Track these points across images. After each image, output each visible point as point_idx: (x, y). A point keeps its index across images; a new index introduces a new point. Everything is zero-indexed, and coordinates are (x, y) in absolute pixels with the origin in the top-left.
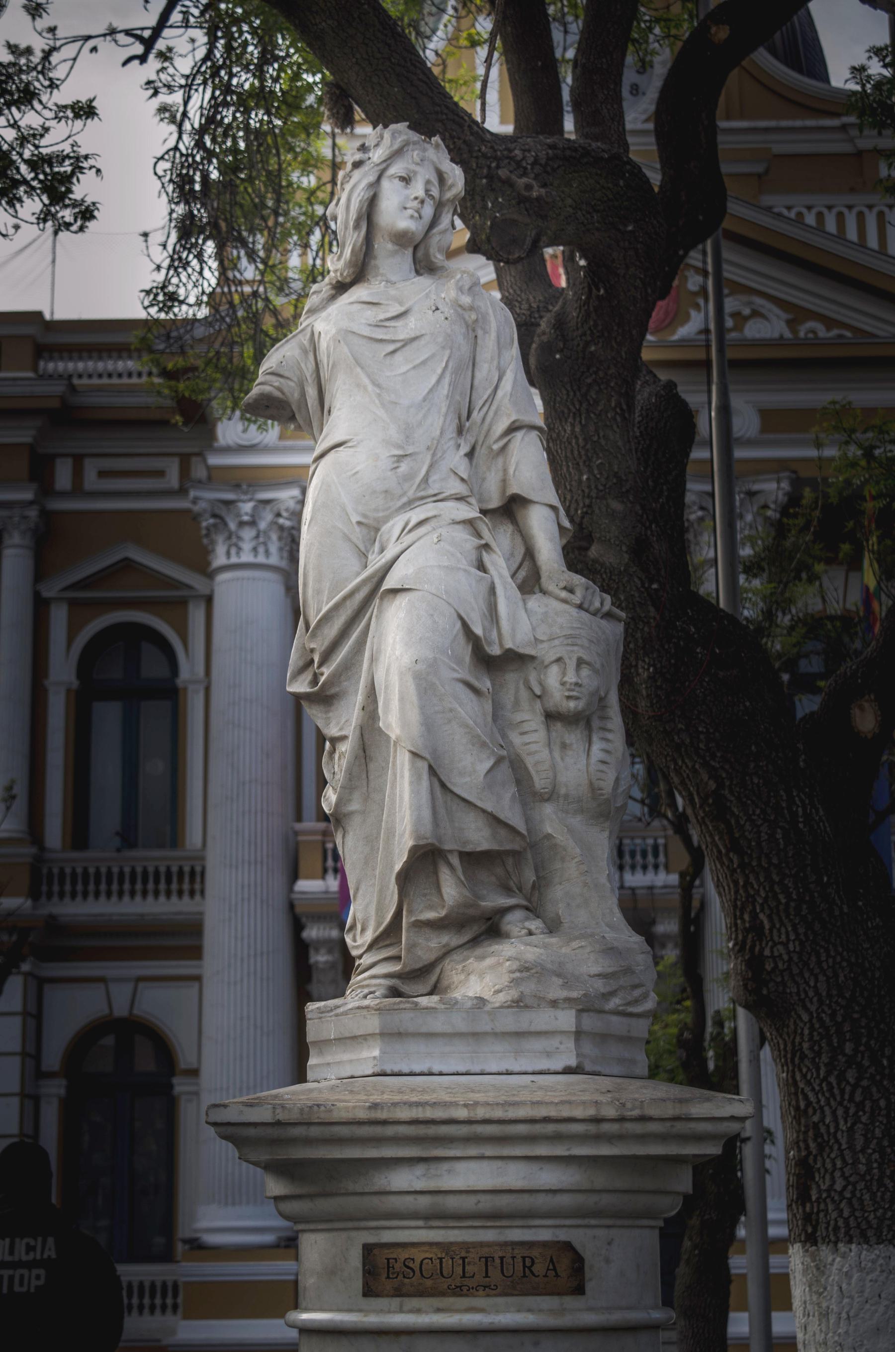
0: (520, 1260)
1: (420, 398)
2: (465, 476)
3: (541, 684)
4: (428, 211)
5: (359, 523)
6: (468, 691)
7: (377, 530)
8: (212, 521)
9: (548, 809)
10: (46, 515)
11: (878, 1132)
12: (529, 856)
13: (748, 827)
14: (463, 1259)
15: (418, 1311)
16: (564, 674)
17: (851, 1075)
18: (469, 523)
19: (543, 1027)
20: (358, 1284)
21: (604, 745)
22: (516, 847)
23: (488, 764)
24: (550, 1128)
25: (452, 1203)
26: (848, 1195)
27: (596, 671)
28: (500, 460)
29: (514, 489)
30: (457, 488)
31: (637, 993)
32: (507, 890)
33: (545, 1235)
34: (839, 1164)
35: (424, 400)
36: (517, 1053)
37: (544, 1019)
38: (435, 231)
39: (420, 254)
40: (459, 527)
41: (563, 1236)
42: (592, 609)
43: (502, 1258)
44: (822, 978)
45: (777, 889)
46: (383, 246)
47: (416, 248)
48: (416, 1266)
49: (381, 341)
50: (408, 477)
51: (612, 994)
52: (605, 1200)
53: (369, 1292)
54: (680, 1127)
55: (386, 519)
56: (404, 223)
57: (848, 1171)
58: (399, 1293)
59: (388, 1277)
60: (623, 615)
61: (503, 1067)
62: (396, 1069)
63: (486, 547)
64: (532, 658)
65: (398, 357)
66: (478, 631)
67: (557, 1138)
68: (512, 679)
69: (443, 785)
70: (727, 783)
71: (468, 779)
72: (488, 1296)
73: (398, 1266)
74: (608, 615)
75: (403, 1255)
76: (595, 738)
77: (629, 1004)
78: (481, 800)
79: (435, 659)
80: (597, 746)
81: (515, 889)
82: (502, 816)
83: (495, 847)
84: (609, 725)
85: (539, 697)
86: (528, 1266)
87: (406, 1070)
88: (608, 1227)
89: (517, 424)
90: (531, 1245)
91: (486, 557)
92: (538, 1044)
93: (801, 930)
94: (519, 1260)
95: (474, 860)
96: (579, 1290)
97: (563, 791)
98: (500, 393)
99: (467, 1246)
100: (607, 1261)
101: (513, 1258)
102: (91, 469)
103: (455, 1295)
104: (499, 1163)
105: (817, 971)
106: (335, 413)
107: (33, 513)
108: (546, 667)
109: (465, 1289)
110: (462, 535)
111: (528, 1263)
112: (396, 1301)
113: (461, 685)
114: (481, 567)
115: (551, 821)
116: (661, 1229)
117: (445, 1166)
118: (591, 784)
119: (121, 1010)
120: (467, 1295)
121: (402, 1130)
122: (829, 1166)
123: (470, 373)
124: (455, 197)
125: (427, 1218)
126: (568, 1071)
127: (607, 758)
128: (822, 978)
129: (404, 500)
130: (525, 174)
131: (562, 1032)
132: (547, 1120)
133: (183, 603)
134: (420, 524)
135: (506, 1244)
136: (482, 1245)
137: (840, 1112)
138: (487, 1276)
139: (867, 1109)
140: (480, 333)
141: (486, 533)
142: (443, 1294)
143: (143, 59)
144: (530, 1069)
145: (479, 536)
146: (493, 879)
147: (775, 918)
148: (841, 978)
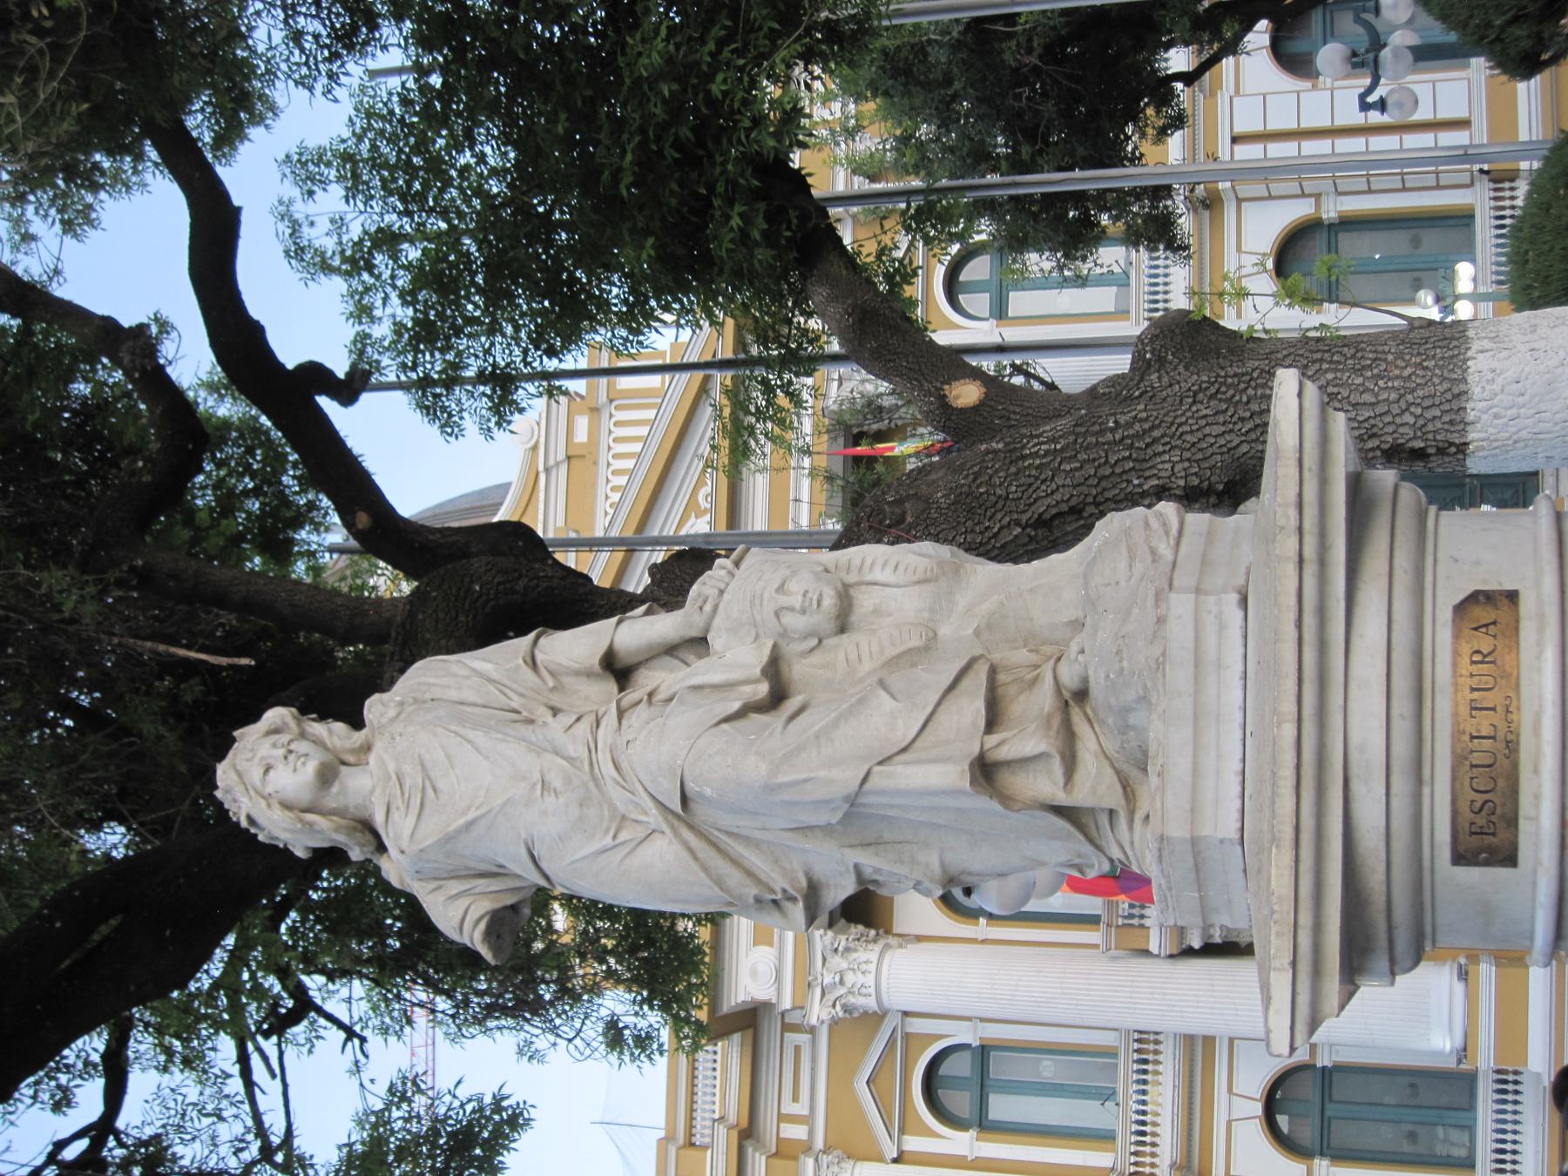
0: (1474, 667)
3: (806, 637)
4: (302, 747)
5: (615, 837)
7: (624, 817)
8: (838, 1007)
9: (945, 631)
10: (827, 1150)
11: (1359, 380)
12: (996, 656)
13: (1057, 496)
14: (1473, 737)
15: (1537, 797)
16: (791, 609)
18: (621, 714)
19: (1191, 634)
20: (1501, 873)
21: (878, 568)
25: (1402, 748)
26: (1419, 411)
27: (794, 573)
29: (595, 661)
30: (584, 728)
31: (1154, 524)
32: (1034, 681)
33: (1445, 634)
34: (1388, 419)
35: (487, 758)
36: (1219, 666)
37: (1179, 632)
39: (351, 759)
41: (1445, 614)
43: (1473, 690)
44: (1207, 430)
45: (1118, 470)
46: (332, 800)
48: (1480, 798)
49: (422, 804)
50: (568, 780)
51: (1153, 552)
52: (1403, 560)
53: (1511, 860)
54: (1310, 460)
56: (310, 769)
57: (1395, 410)
58: (1512, 822)
59: (1493, 834)
60: (741, 547)
61: (1239, 684)
62: (1236, 815)
63: (650, 695)
64: (775, 646)
65: (441, 785)
66: (736, 706)
67: (1322, 611)
68: (799, 670)
69: (904, 750)
70: (1015, 516)
72: (1518, 709)
73: (1481, 821)
74: (737, 564)
75: (1466, 815)
76: (869, 578)
77: (1167, 533)
80: (878, 575)
83: (983, 691)
84: (857, 562)
85: (820, 641)
86: (1484, 658)
87: (1238, 803)
88: (1435, 561)
89: (529, 659)
90: (1456, 653)
92: (1210, 639)
93: (1161, 449)
94: (1475, 669)
95: (993, 721)
96: (1512, 596)
97: (926, 615)
98: (495, 675)
99: (1457, 734)
100: (1477, 563)
101: (1472, 675)
104: (1353, 686)
105: (1200, 435)
106: (502, 861)
109: (1510, 737)
110: (635, 718)
111: (1477, 658)
112: (1523, 825)
113: (791, 725)
115: (958, 631)
116: (1440, 509)
117: (1354, 756)
118: (919, 582)
119: (1258, 1109)
120: (1518, 735)
122: (1390, 429)
123: (469, 709)
125: (1419, 780)
127: (892, 564)
128: (1207, 430)
129: (591, 785)
132: (1299, 624)
135: (1455, 684)
136: (1455, 715)
138: (1493, 709)
139: (1336, 390)
140: (428, 696)
143: (363, 1040)
144: (1241, 650)
146: (1022, 698)
147: (1148, 473)
148: (1208, 412)
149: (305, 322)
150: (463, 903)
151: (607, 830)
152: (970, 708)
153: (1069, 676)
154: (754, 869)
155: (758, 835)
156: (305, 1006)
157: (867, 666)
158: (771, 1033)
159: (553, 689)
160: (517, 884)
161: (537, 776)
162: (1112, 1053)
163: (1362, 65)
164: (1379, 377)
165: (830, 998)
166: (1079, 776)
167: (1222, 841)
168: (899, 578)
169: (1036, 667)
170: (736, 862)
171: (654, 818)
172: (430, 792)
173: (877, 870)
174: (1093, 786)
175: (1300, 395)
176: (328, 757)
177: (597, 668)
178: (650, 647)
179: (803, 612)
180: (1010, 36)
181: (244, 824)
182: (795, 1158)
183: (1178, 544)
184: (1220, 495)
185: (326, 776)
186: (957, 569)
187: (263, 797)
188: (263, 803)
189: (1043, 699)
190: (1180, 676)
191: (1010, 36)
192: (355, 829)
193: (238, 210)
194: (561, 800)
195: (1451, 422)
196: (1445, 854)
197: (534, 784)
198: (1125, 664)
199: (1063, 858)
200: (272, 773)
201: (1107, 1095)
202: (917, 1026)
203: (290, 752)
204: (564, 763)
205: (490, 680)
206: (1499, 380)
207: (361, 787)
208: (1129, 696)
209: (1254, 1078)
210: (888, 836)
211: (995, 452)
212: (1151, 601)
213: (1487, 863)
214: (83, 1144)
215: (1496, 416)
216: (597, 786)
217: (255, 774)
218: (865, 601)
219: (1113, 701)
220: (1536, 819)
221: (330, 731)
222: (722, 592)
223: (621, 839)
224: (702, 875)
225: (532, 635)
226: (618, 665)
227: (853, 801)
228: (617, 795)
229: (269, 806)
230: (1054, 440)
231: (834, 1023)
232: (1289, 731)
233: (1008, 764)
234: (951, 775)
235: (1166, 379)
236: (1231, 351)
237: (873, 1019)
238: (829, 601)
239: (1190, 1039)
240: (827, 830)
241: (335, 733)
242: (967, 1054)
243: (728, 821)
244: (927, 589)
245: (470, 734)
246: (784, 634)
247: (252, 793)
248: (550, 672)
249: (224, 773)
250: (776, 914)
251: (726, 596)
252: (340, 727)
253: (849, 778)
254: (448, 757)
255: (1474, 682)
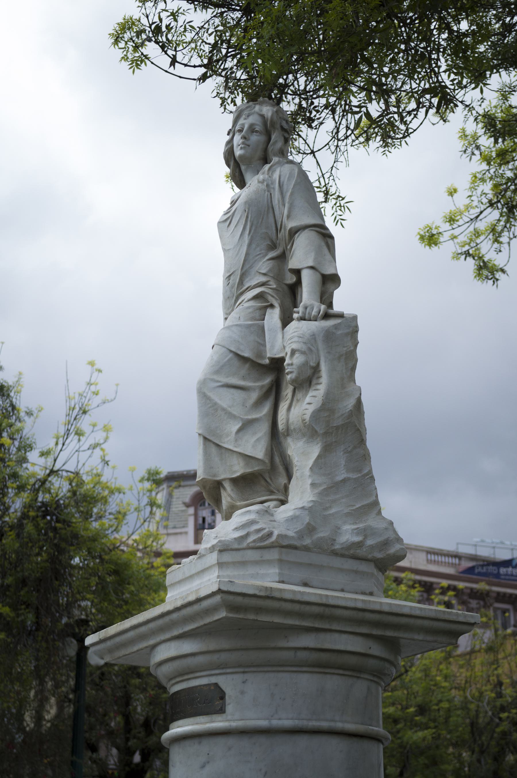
2: (264, 271)
6: (232, 391)
23: (235, 427)
69: (218, 445)
71: (229, 438)
78: (236, 447)
81: (275, 491)
83: (249, 470)
88: (244, 672)
113: (225, 389)
123: (271, 215)
129: (234, 298)
152: (239, 469)
169: (278, 491)
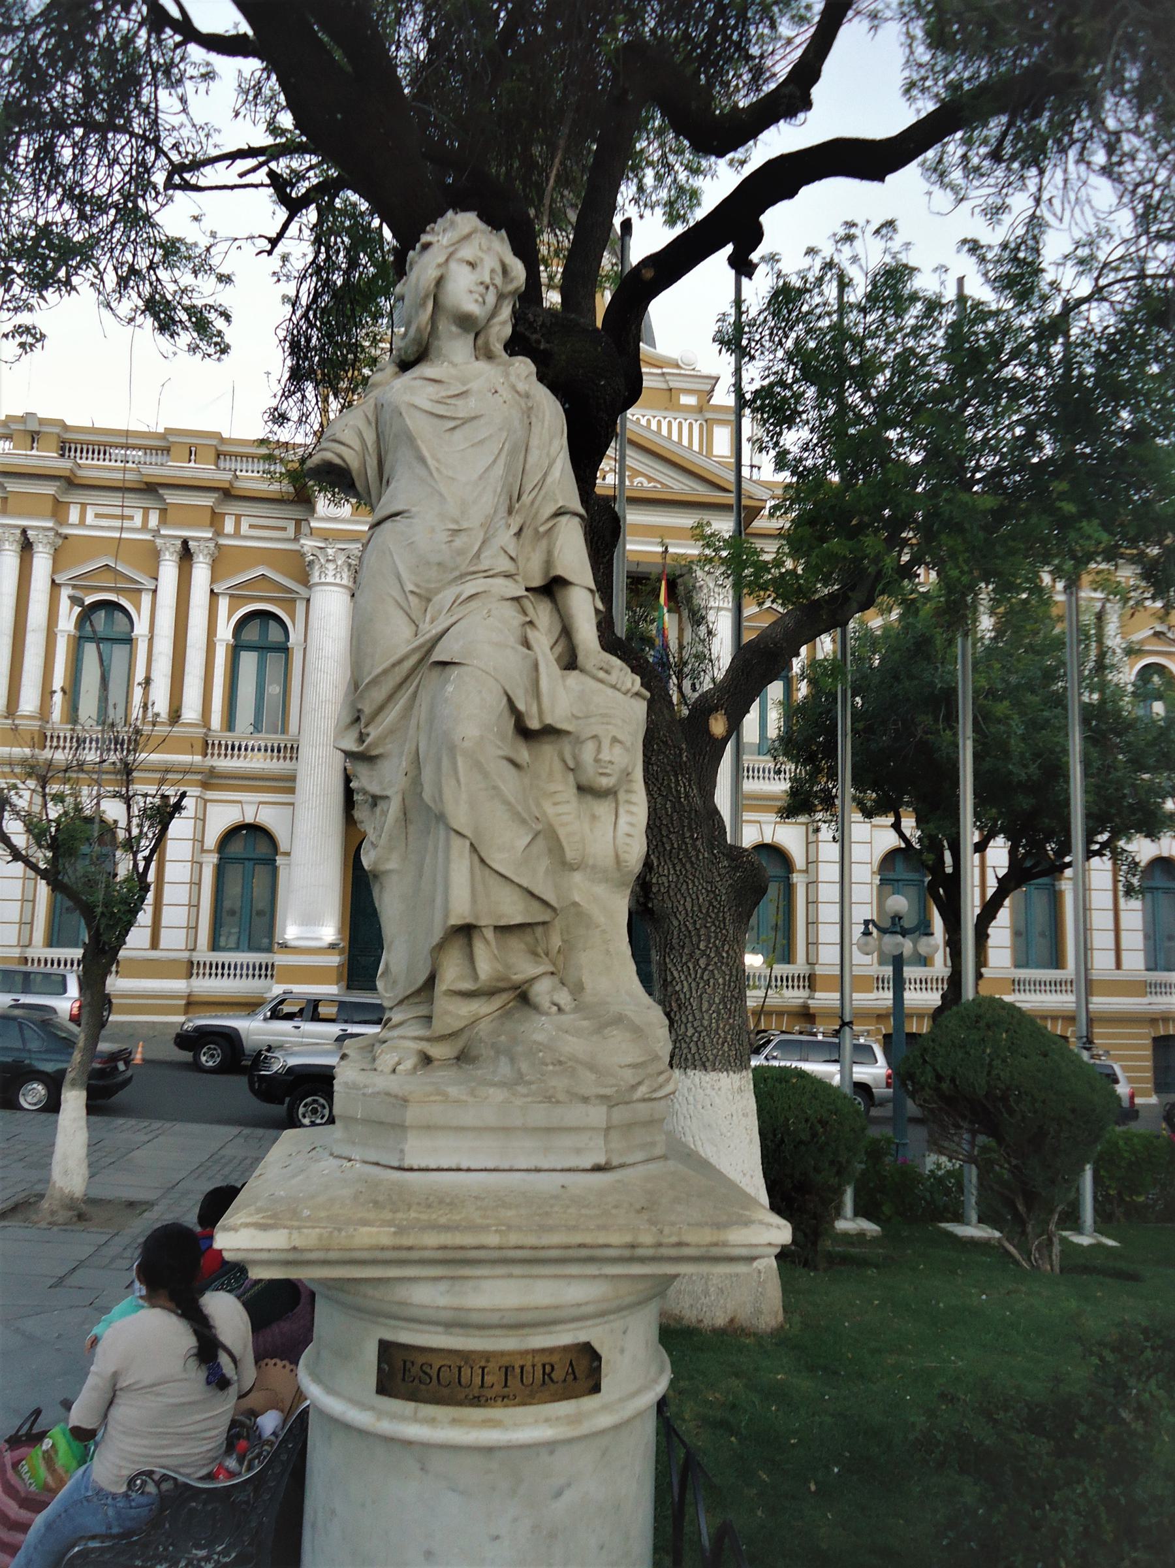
1: (475, 476)
3: (575, 757)
4: (491, 298)
5: (412, 592)
7: (429, 600)
9: (577, 877)
14: (483, 1369)
15: (432, 1421)
16: (599, 750)
17: (702, 962)
18: (517, 599)
22: (546, 918)
24: (584, 1253)
27: (627, 750)
28: (544, 544)
29: (559, 571)
30: (507, 566)
32: (535, 954)
35: (480, 478)
37: (576, 1114)
38: (495, 320)
39: (480, 342)
40: (509, 603)
41: (582, 1338)
42: (624, 689)
43: (522, 1368)
46: (446, 327)
47: (477, 335)
50: (460, 552)
51: (640, 1083)
53: (384, 1388)
55: (437, 591)
56: (471, 306)
58: (413, 1397)
60: (648, 694)
61: (532, 1166)
62: (423, 1165)
63: (531, 622)
64: (568, 733)
65: (458, 433)
66: (521, 706)
68: (548, 750)
69: (482, 861)
72: (506, 1406)
73: (415, 1370)
75: (421, 1359)
76: (621, 811)
77: (655, 1091)
79: (482, 737)
80: (623, 819)
82: (536, 892)
84: (634, 798)
87: (433, 1166)
91: (532, 635)
92: (567, 1141)
95: (504, 930)
97: (591, 862)
98: (549, 480)
99: (487, 1356)
102: (90, 513)
103: (472, 1405)
106: (393, 485)
107: (211, 545)
108: (583, 742)
109: (483, 1400)
110: (510, 612)
111: (548, 1369)
112: (411, 1405)
113: (505, 763)
114: (527, 644)
117: (471, 1283)
118: (617, 856)
119: (249, 819)
121: (427, 1254)
124: (517, 289)
126: (597, 1168)
129: (457, 573)
130: (535, 332)
131: (593, 1129)
132: (580, 1246)
133: (294, 600)
134: (471, 597)
135: (527, 1352)
136: (502, 1354)
137: (693, 985)
140: (534, 420)
141: (530, 610)
142: (460, 1403)
143: (270, 253)
144: (559, 1167)
145: (525, 614)
146: (523, 946)
149: (795, 230)
150: (356, 444)
151: (417, 586)
152: (514, 911)
153: (542, 991)
154: (386, 711)
155: (413, 722)
156: (294, 207)
157: (550, 810)
158: (296, 512)
159: (536, 531)
160: (374, 492)
161: (465, 525)
162: (284, 730)
163: (894, 924)
164: (719, 1013)
165: (318, 552)
166: (458, 1000)
167: (402, 1151)
168: (620, 841)
169: (547, 954)
170: (391, 697)
171: (430, 630)
172: (452, 424)
173: (385, 813)
174: (453, 1013)
175: (770, 1244)
176: (482, 323)
177: (554, 573)
178: (570, 617)
179: (597, 760)
180: (936, 720)
181: (425, 238)
182: (212, 525)
183: (644, 1100)
184: (645, 904)
185: (465, 322)
186: (624, 884)
187: (447, 260)
188: (441, 259)
189: (524, 968)
190: (539, 1115)
191: (936, 720)
192: (420, 344)
193: (882, 180)
194: (444, 547)
195: (686, 1059)
196: (389, 1336)
197: (457, 522)
198: (551, 1068)
199: (394, 969)
200: (468, 268)
201: (257, 727)
202: (300, 607)
203: (487, 288)
204: (476, 548)
205: (545, 475)
206: (713, 1093)
207: (456, 351)
208: (524, 1066)
209: (267, 817)
210: (411, 828)
211: (681, 755)
212: (603, 1091)
213: (380, 1370)
214: (175, 13)
215: (689, 1090)
216: (455, 579)
217: (467, 252)
218: (603, 809)
219: (520, 1049)
220: (415, 1419)
221: (504, 323)
222: (614, 687)
223: (411, 598)
224: (379, 670)
225: (582, 511)
226: (555, 588)
227: (441, 817)
228: (448, 595)
229: (439, 266)
230: (687, 796)
231: (303, 555)
232: (492, 1239)
233: (470, 945)
234: (460, 911)
235: (723, 871)
236: (740, 914)
237: (305, 581)
238: (605, 782)
239: (292, 778)
240: (416, 781)
241: (502, 328)
242: (282, 639)
243: (424, 699)
244: (610, 862)
245: (502, 462)
246: (578, 741)
247: (451, 249)
248: (550, 529)
249: (467, 221)
250: (348, 720)
251: (610, 691)
252: (508, 331)
253: (459, 817)
254: (481, 442)
255: (528, 1368)
